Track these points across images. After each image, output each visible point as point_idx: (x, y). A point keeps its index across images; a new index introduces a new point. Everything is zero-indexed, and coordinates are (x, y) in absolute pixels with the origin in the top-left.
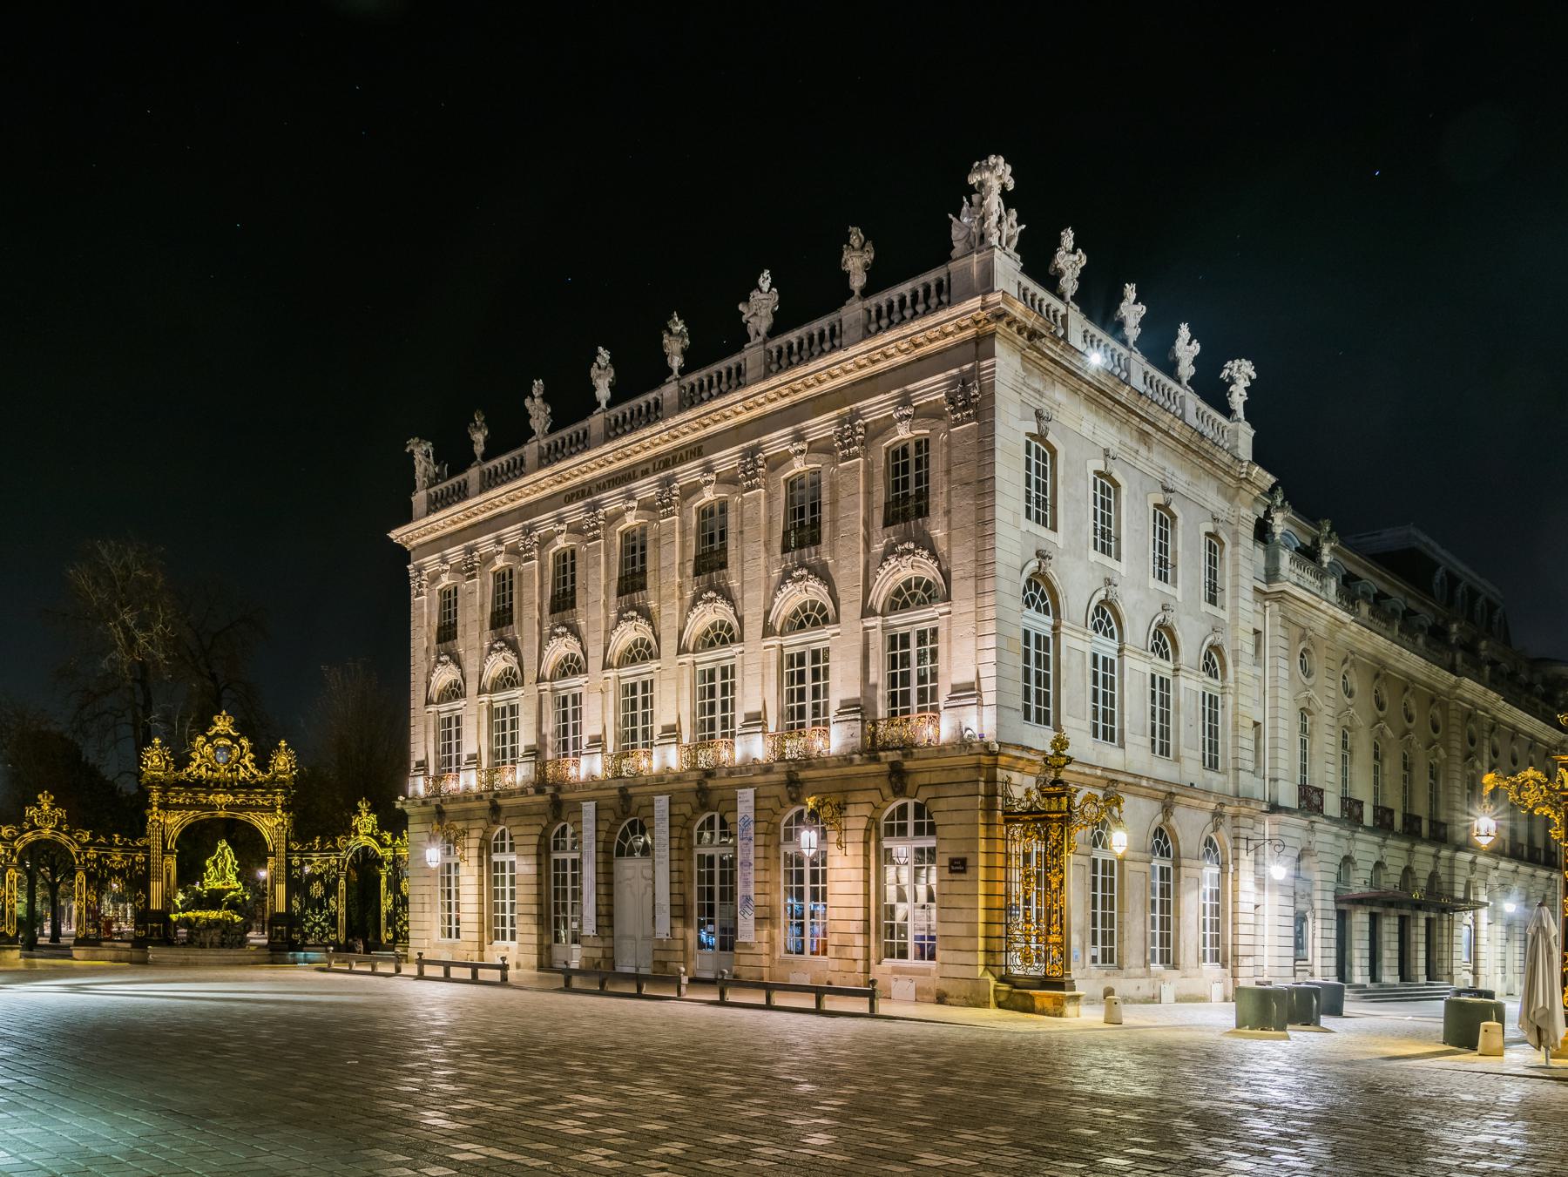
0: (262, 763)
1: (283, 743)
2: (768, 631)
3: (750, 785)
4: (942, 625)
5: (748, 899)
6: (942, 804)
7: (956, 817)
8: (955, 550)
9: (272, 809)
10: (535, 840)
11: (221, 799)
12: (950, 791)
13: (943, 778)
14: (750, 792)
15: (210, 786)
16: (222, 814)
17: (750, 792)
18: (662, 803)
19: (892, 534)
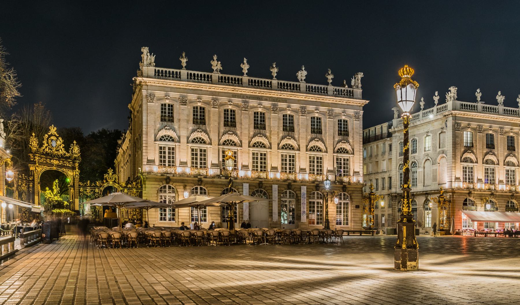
0: (67, 148)
1: (75, 142)
2: (307, 150)
3: (305, 185)
4: (351, 159)
5: (304, 212)
6: (354, 195)
7: (357, 197)
8: (355, 145)
9: (73, 168)
10: (220, 192)
11: (55, 162)
12: (356, 192)
13: (354, 189)
14: (305, 187)
15: (51, 156)
16: (54, 168)
17: (305, 187)
18: (275, 187)
19: (341, 138)
